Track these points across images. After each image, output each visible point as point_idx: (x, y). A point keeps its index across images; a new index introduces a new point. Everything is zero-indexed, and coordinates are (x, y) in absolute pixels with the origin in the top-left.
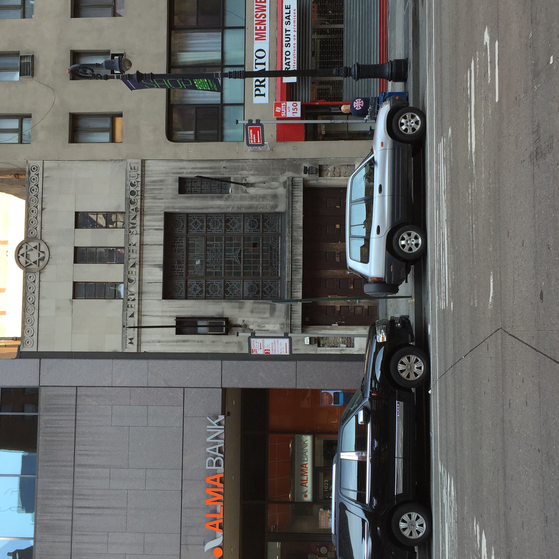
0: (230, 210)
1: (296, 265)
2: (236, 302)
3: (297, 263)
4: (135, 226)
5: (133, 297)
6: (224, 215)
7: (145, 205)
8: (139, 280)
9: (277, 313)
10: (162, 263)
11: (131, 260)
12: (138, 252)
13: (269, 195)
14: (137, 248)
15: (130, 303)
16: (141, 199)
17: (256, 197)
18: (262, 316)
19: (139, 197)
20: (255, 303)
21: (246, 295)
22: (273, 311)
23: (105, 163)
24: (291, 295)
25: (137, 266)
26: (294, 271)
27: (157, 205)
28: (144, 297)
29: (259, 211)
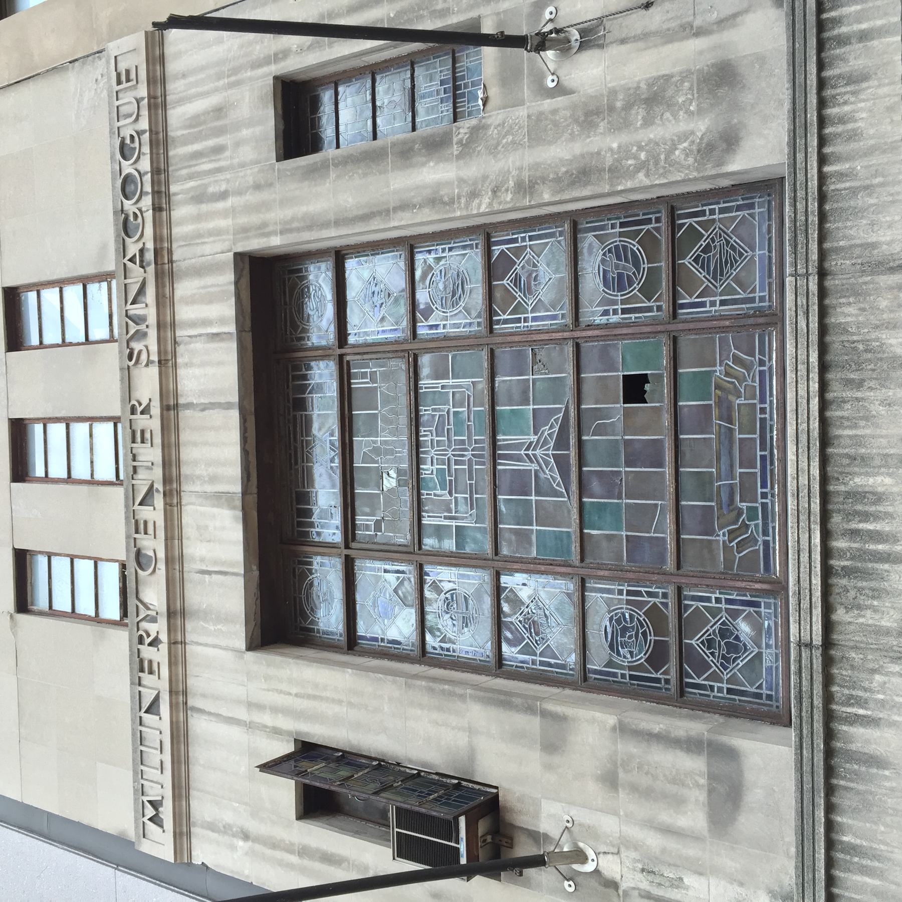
0: (482, 208)
1: (854, 534)
2: (530, 710)
3: (866, 517)
4: (142, 327)
5: (153, 628)
6: (480, 241)
7: (176, 231)
8: (169, 561)
9: (748, 822)
10: (237, 488)
11: (142, 474)
12: (158, 440)
13: (686, 75)
14: (152, 423)
15: (148, 652)
16: (157, 209)
17: (611, 109)
18: (666, 817)
19: (147, 202)
20: (623, 730)
21: (596, 664)
22: (726, 795)
23: (56, 81)
24: (829, 735)
25: (159, 500)
26: (848, 572)
27: (211, 225)
28: (194, 630)
29: (639, 184)
